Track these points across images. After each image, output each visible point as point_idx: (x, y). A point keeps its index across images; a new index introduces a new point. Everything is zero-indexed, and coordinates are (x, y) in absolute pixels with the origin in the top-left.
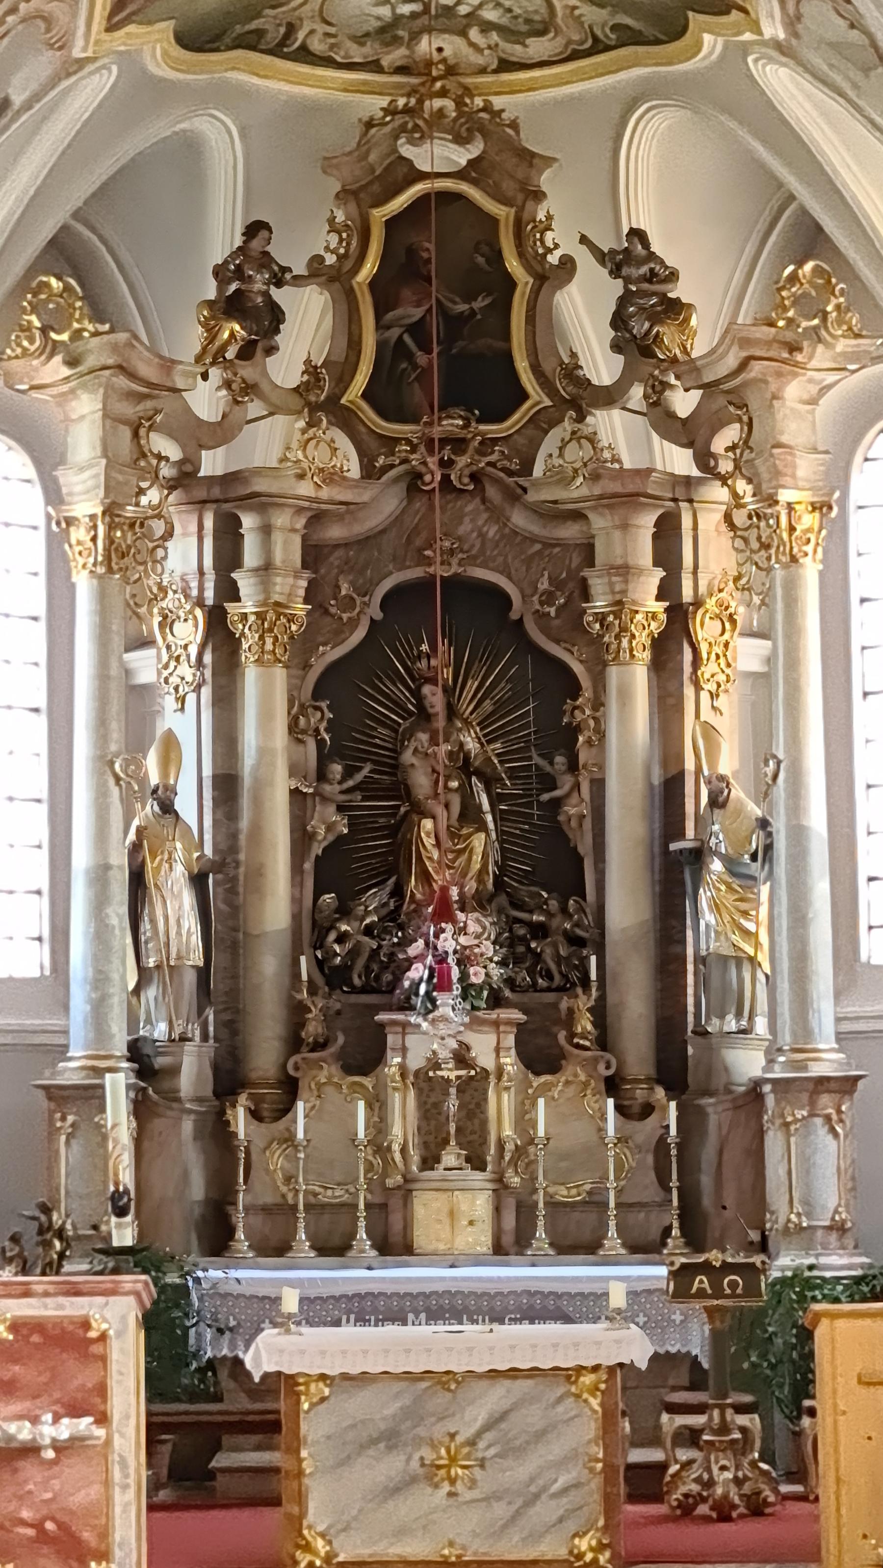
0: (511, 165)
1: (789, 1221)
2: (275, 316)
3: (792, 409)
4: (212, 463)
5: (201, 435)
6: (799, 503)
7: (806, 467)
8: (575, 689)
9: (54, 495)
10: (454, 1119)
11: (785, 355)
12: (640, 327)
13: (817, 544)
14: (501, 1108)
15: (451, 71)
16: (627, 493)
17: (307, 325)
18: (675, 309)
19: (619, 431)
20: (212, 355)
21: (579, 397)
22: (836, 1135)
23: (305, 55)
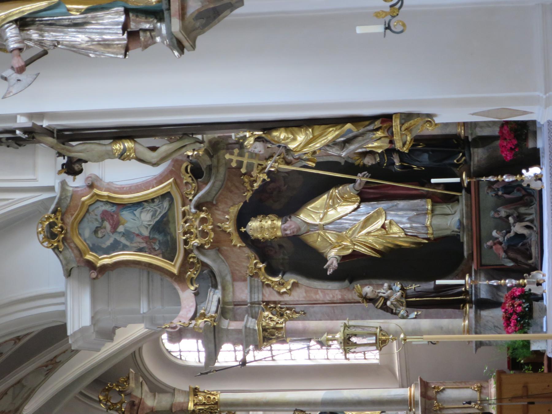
1: (478, 409)
3: (157, 403)
6: (194, 401)
11: (136, 408)
13: (210, 394)
22: (444, 389)
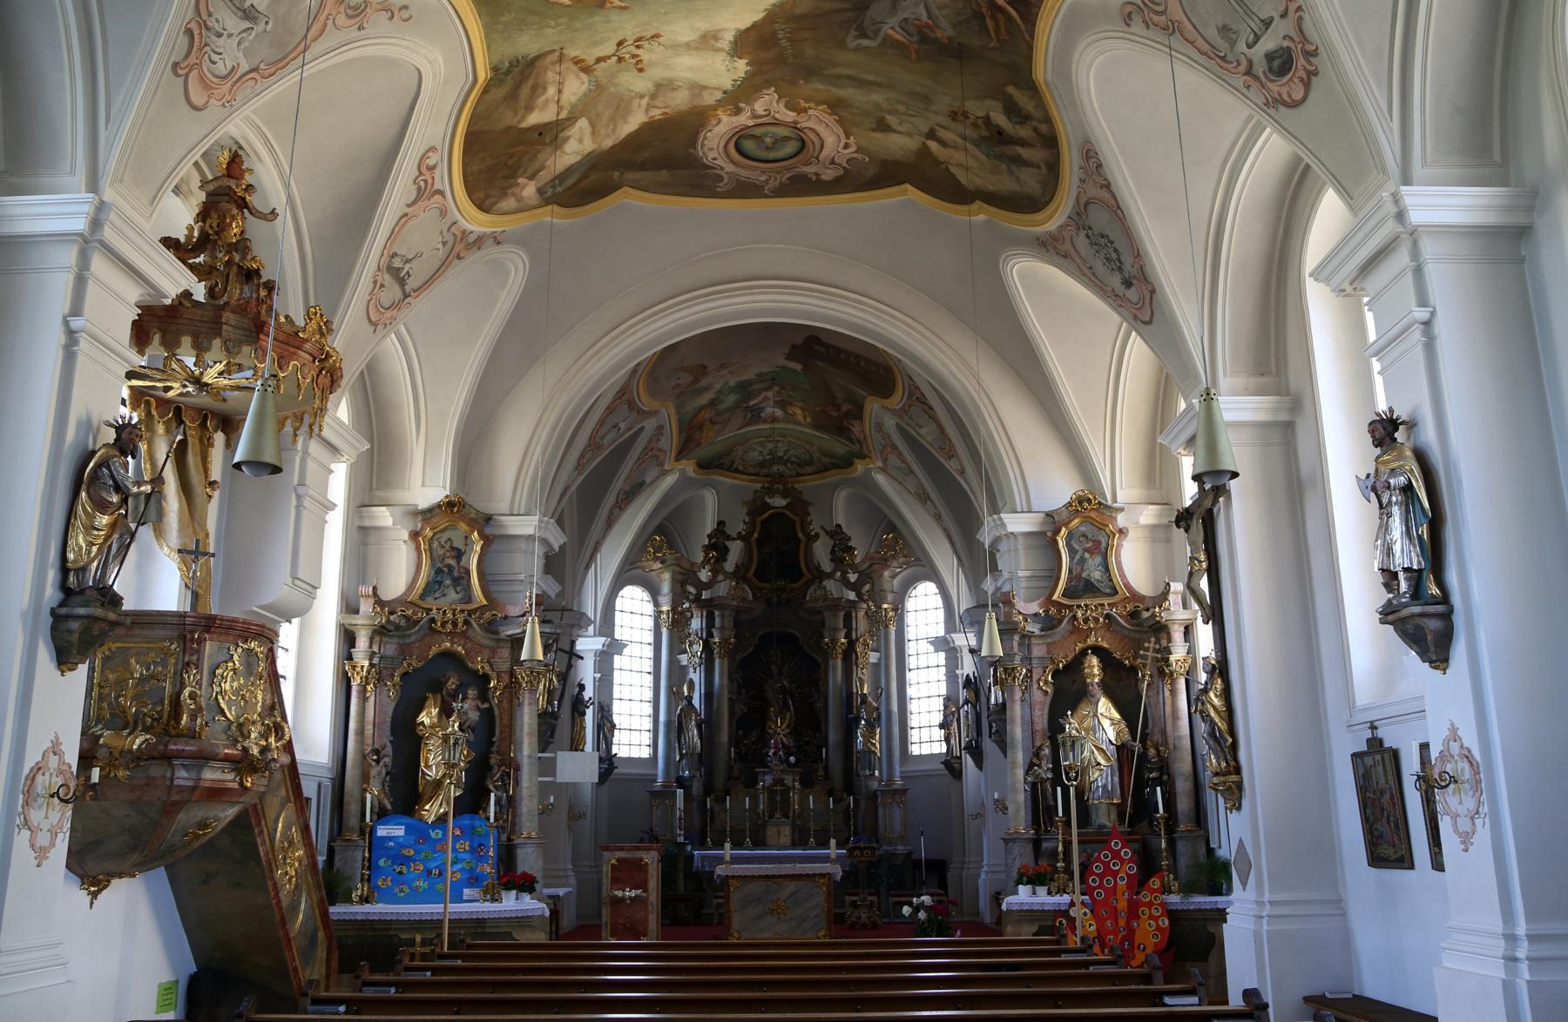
0: (800, 505)
2: (727, 550)
4: (705, 595)
5: (702, 586)
7: (890, 597)
8: (818, 666)
9: (656, 604)
10: (779, 802)
12: (839, 554)
14: (795, 798)
15: (782, 476)
16: (836, 604)
17: (736, 549)
18: (851, 549)
19: (831, 586)
20: (706, 561)
21: (821, 575)
23: (737, 471)
